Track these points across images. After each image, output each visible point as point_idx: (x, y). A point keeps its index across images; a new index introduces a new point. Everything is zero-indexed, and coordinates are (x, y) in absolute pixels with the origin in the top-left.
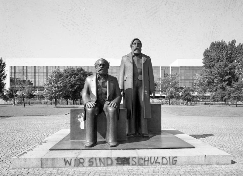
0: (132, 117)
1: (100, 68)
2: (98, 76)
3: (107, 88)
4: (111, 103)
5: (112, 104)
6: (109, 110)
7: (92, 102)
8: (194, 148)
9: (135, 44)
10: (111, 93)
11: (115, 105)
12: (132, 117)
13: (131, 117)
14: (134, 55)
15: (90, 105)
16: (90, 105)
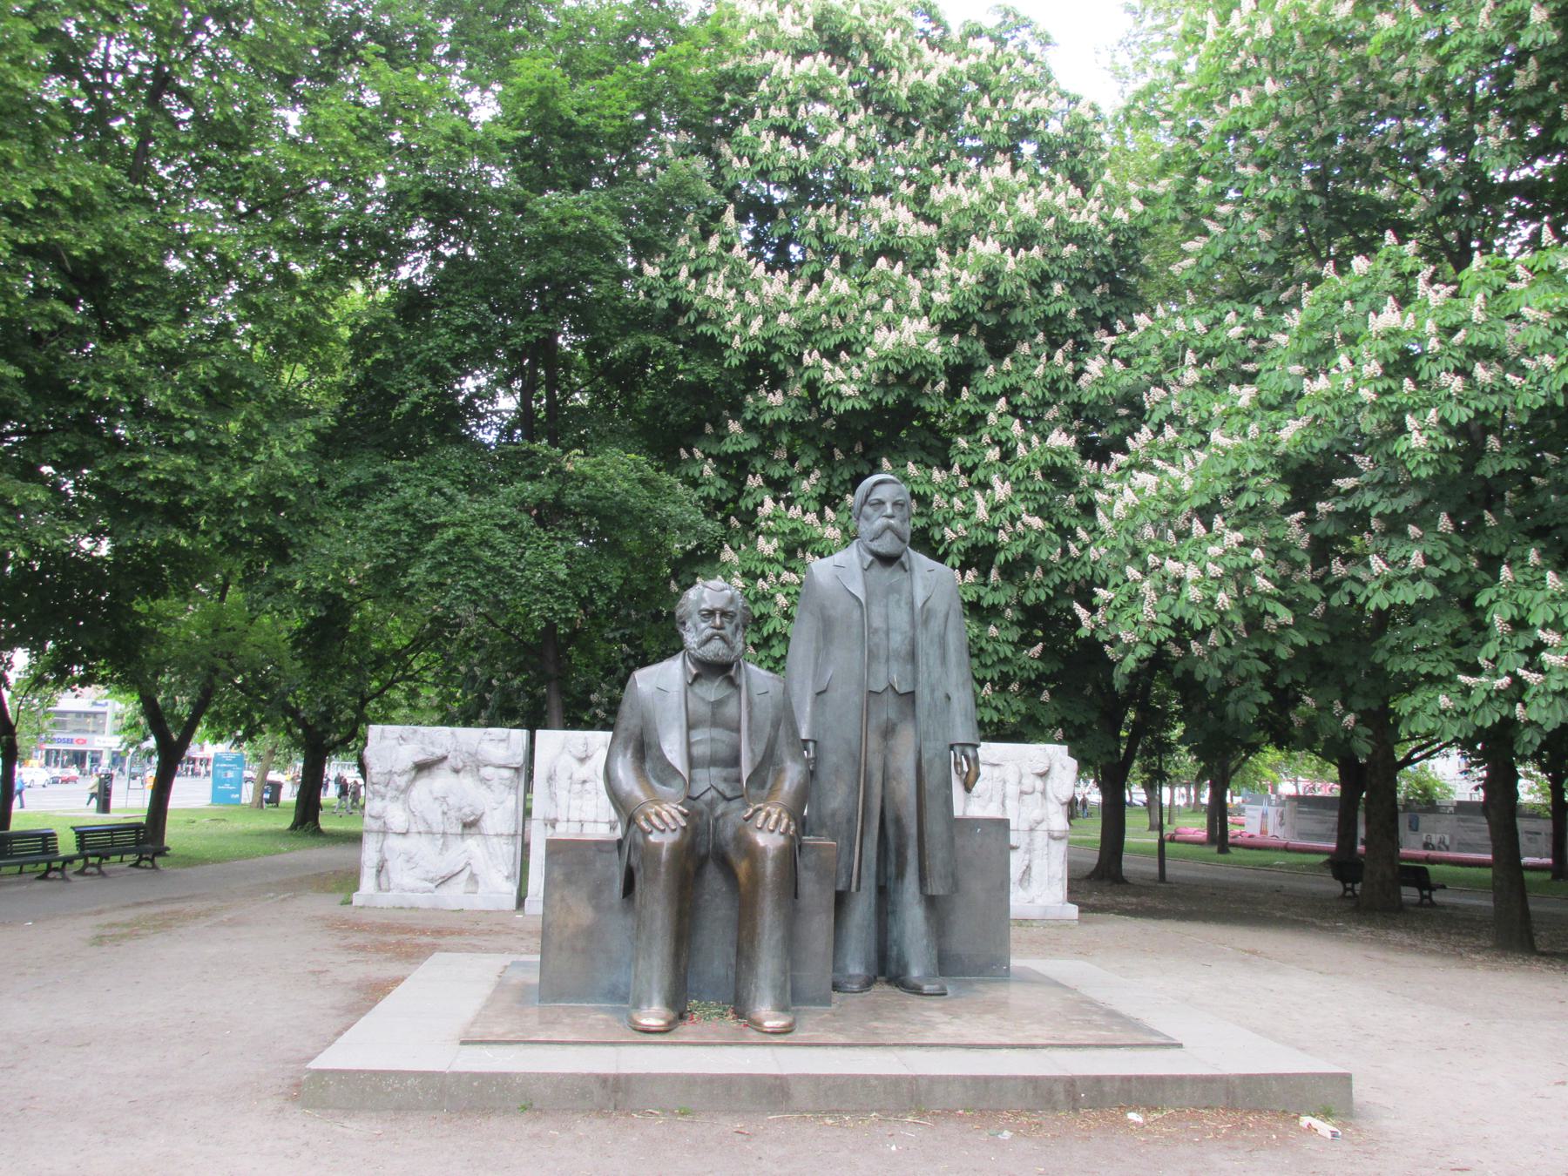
0: (858, 889)
1: (709, 632)
2: (694, 671)
3: (738, 730)
4: (760, 809)
5: (768, 815)
6: (752, 853)
7: (666, 806)
8: (1180, 1046)
9: (881, 503)
10: (759, 759)
11: (785, 821)
12: (858, 889)
13: (853, 889)
14: (872, 563)
15: (658, 815)
16: (658, 815)
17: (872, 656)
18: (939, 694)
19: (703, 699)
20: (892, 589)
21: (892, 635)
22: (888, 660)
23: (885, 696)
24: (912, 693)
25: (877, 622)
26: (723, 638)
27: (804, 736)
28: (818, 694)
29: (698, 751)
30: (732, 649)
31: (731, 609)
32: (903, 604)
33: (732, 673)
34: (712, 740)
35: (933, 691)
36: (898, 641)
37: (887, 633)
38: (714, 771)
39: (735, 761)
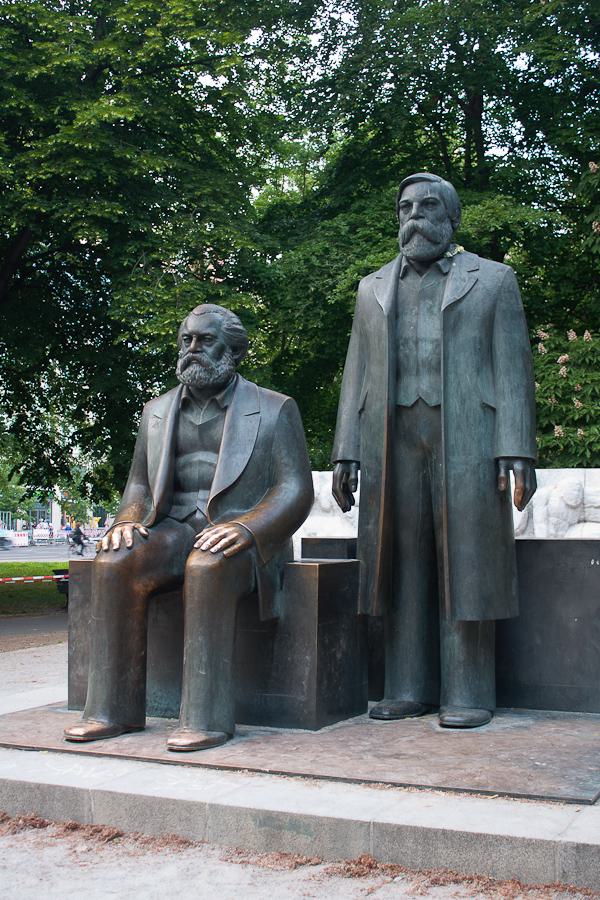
9: (409, 205)
17: (397, 372)
18: (474, 403)
19: (191, 423)
20: (423, 295)
21: (422, 345)
22: (418, 371)
23: (417, 410)
24: (437, 407)
25: (408, 333)
26: (199, 362)
27: (350, 457)
28: (360, 413)
29: (193, 473)
30: (211, 371)
31: (209, 331)
32: (435, 310)
33: (218, 397)
34: (201, 463)
35: (463, 402)
36: (426, 350)
37: (416, 343)
38: (201, 494)
39: (208, 486)
